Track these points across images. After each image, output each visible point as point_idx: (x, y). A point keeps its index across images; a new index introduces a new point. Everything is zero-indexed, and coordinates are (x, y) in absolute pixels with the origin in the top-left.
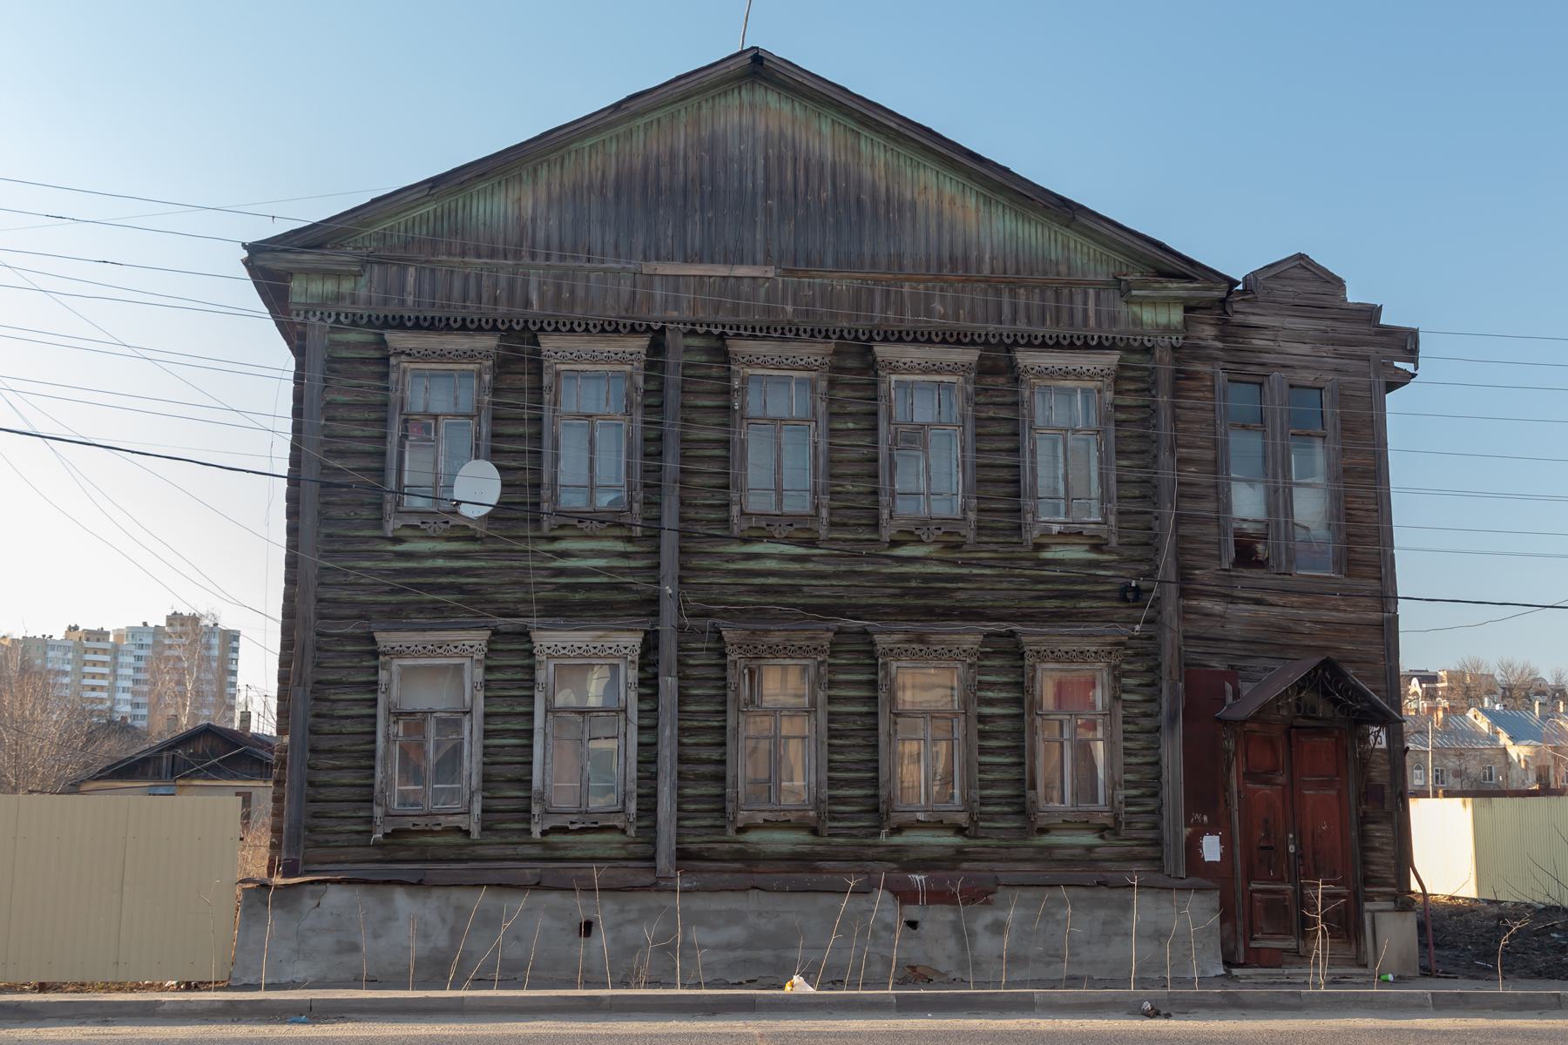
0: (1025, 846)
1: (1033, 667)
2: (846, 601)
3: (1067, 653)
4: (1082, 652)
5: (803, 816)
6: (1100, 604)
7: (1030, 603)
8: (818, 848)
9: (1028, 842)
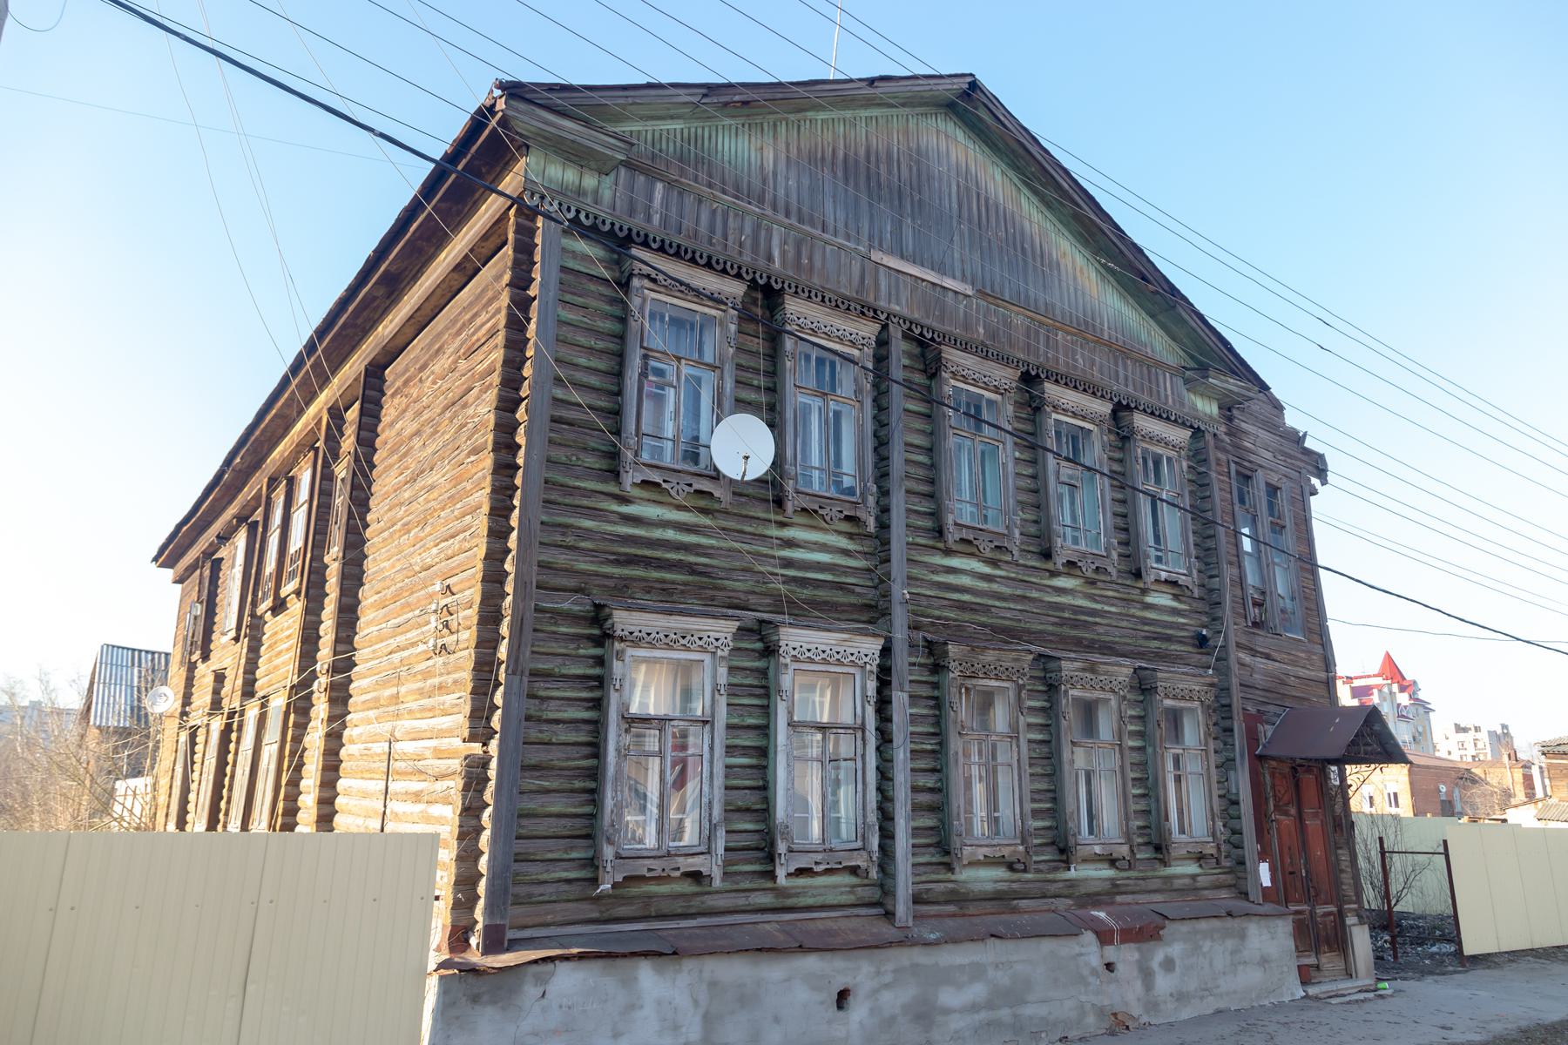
0: (1153, 877)
2: (1022, 625)
5: (1015, 852)
8: (1015, 886)
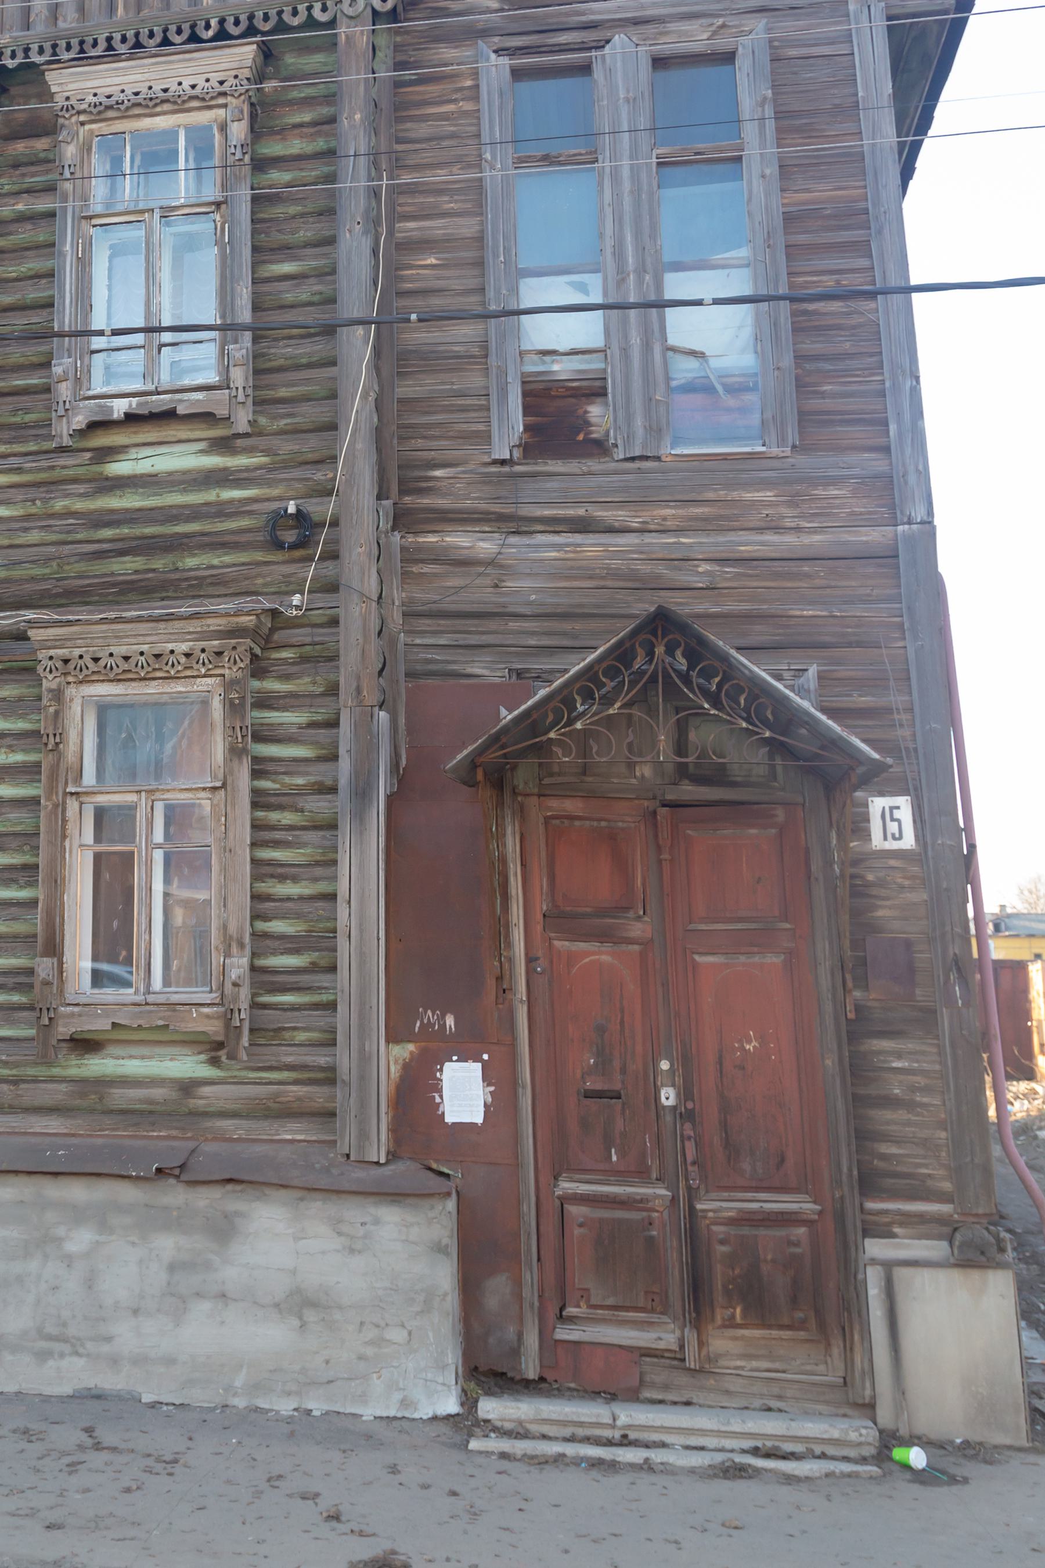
0: (53, 1080)
1: (58, 695)
3: (126, 658)
4: (157, 656)
6: (227, 559)
7: (82, 567)
9: (56, 1071)
